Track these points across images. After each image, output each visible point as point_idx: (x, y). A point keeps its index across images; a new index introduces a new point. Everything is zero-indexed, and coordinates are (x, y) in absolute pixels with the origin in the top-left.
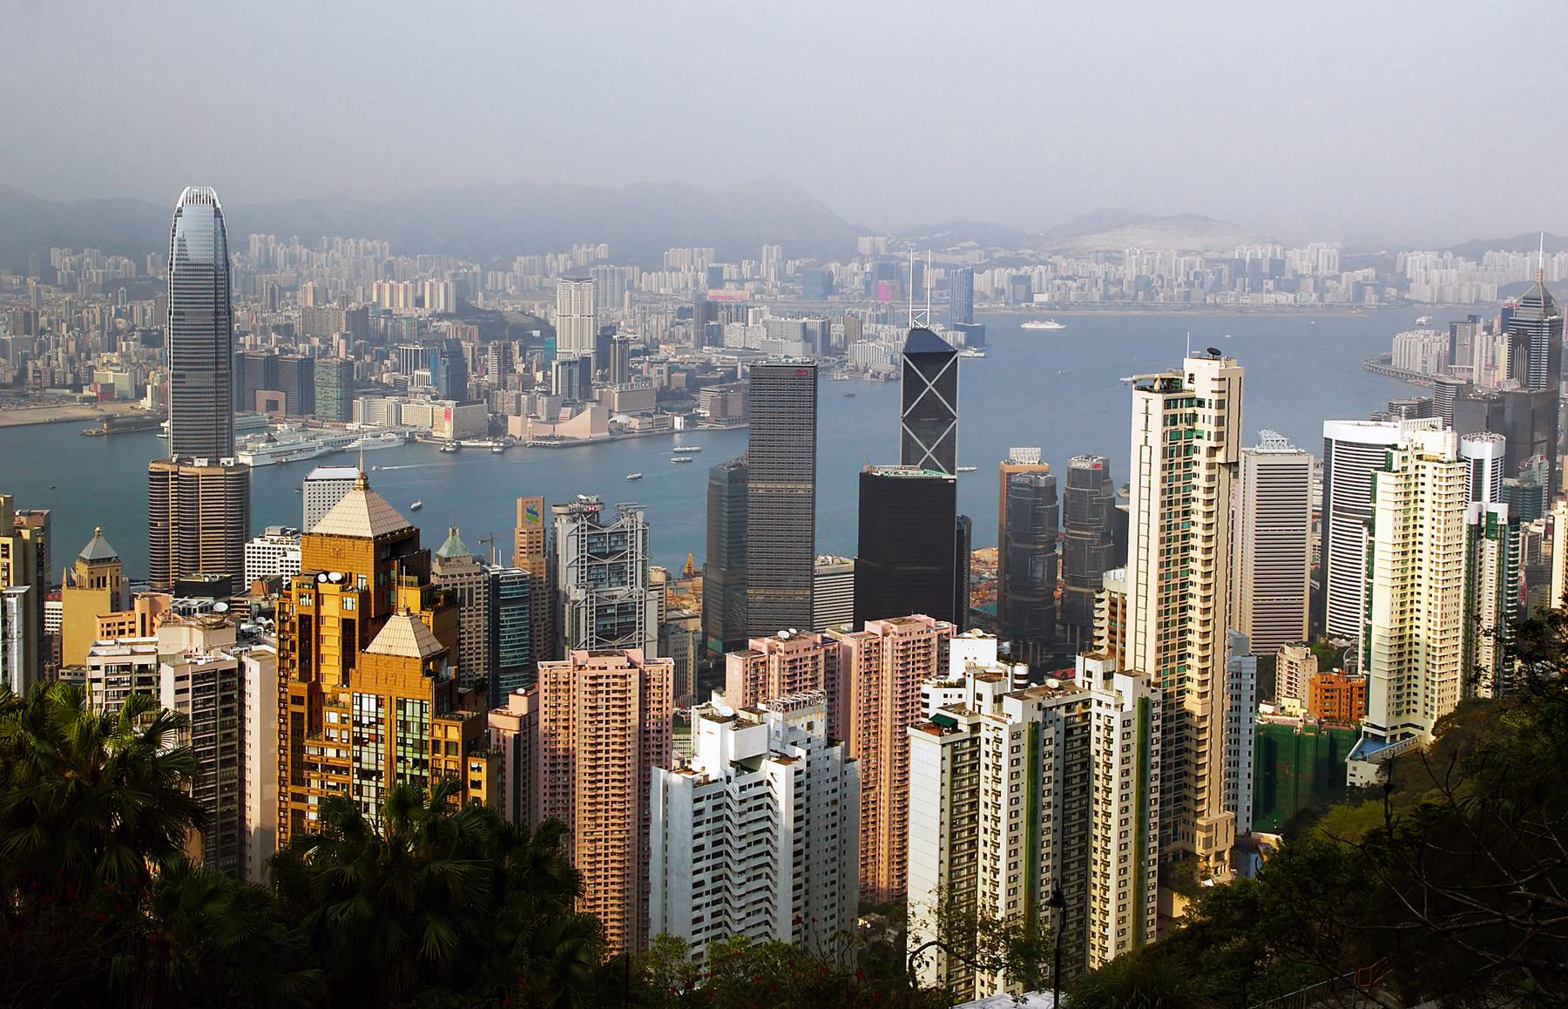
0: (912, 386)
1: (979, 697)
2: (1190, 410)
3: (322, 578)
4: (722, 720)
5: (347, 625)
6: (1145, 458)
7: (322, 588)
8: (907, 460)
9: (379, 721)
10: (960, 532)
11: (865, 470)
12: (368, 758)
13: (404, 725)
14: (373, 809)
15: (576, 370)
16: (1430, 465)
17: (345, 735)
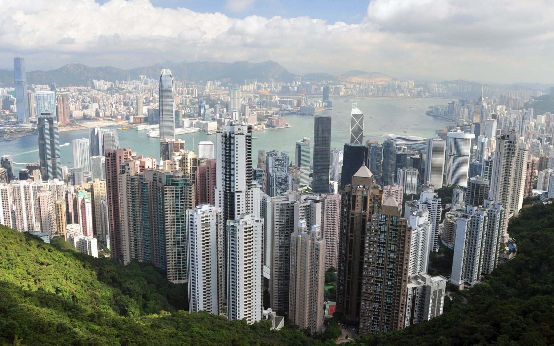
0: (353, 122)
1: (471, 210)
2: (509, 144)
3: (358, 187)
4: (416, 216)
5: (365, 198)
6: (499, 154)
7: (358, 189)
8: (352, 141)
9: (387, 221)
10: (369, 160)
11: (344, 144)
12: (383, 228)
13: (392, 221)
14: (383, 240)
15: (237, 113)
16: (521, 151)
17: (376, 224)
